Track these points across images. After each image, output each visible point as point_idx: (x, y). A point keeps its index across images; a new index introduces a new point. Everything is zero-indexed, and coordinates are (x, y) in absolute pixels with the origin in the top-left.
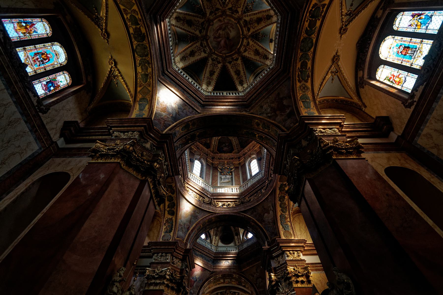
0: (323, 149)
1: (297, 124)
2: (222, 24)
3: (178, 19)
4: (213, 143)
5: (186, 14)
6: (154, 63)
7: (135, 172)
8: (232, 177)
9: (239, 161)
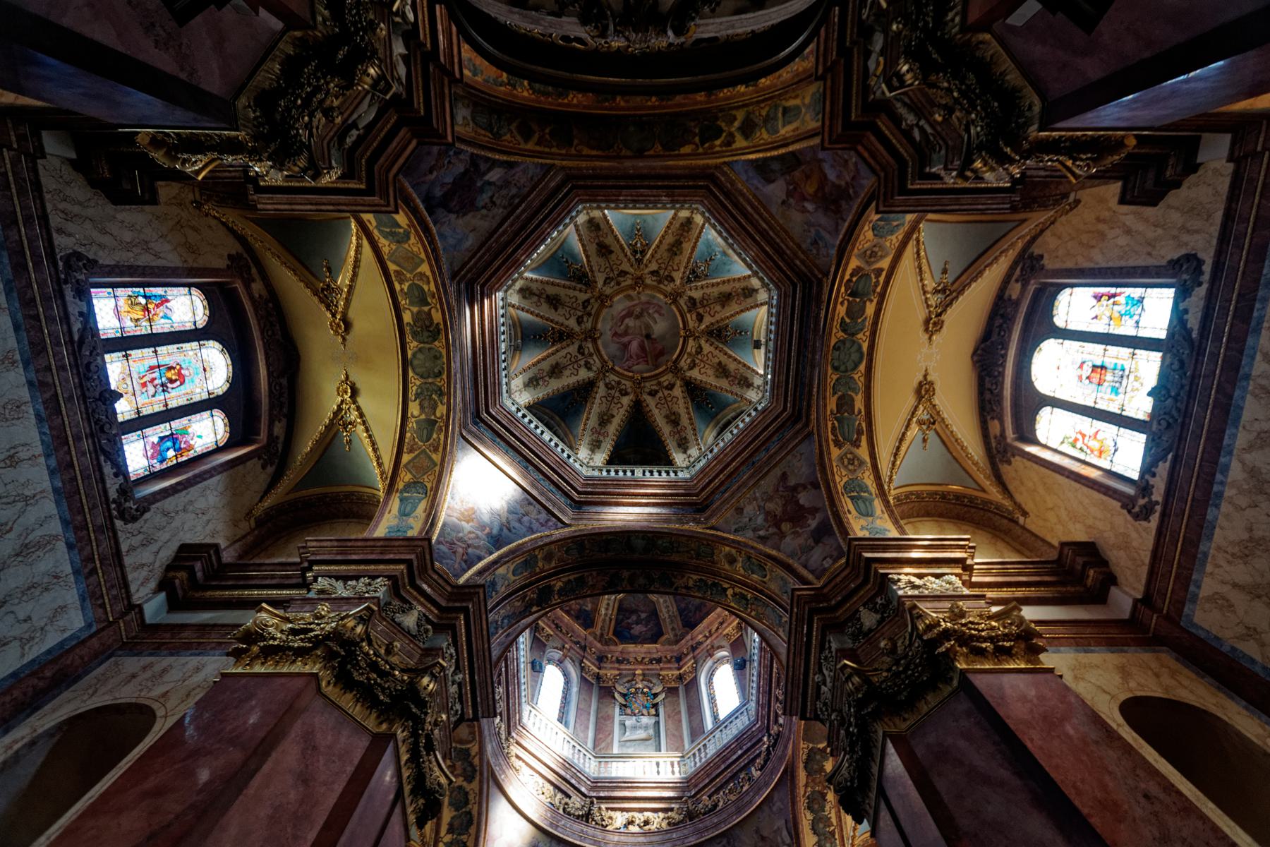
0: (925, 638)
1: (843, 560)
3: (525, 292)
4: (603, 611)
5: (547, 283)
6: (455, 392)
7: (358, 708)
8: (657, 723)
9: (679, 669)
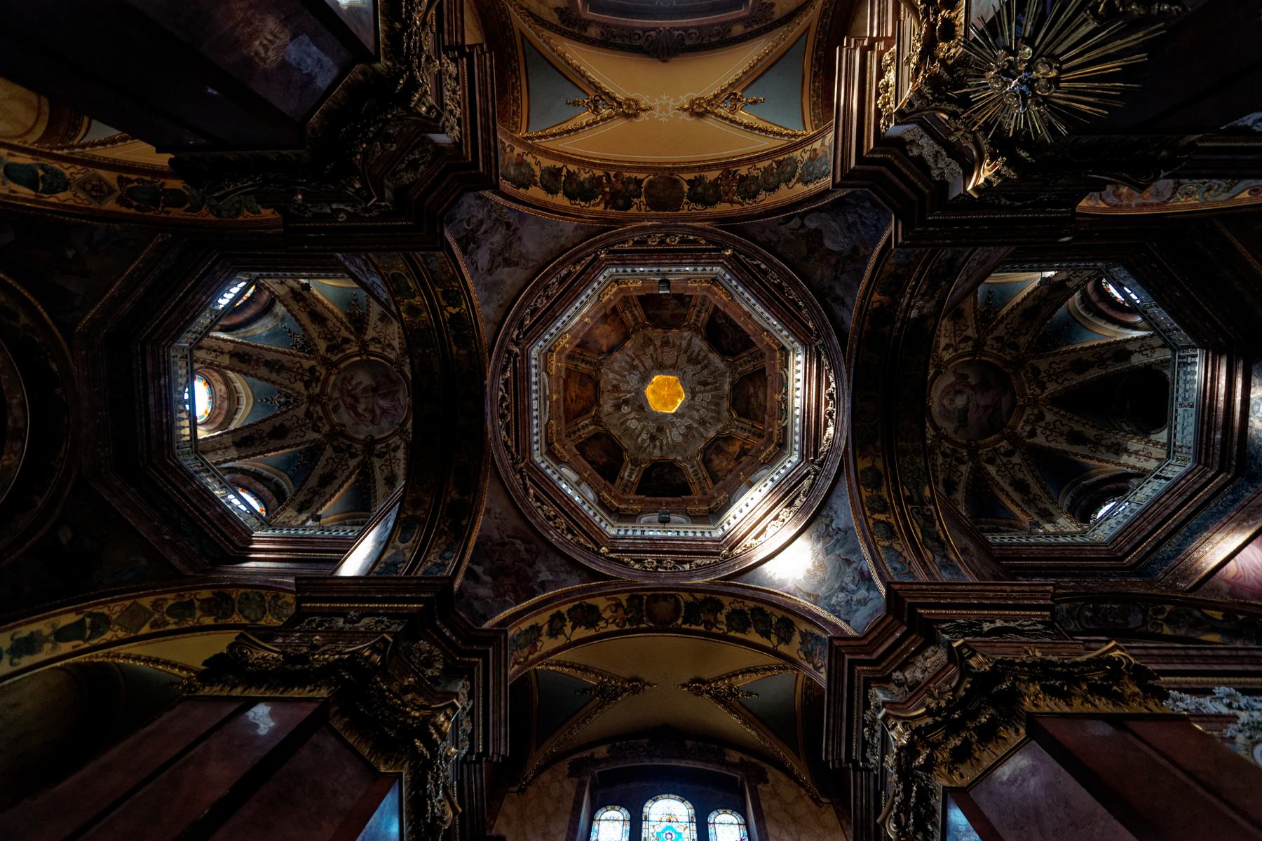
2: (344, 402)
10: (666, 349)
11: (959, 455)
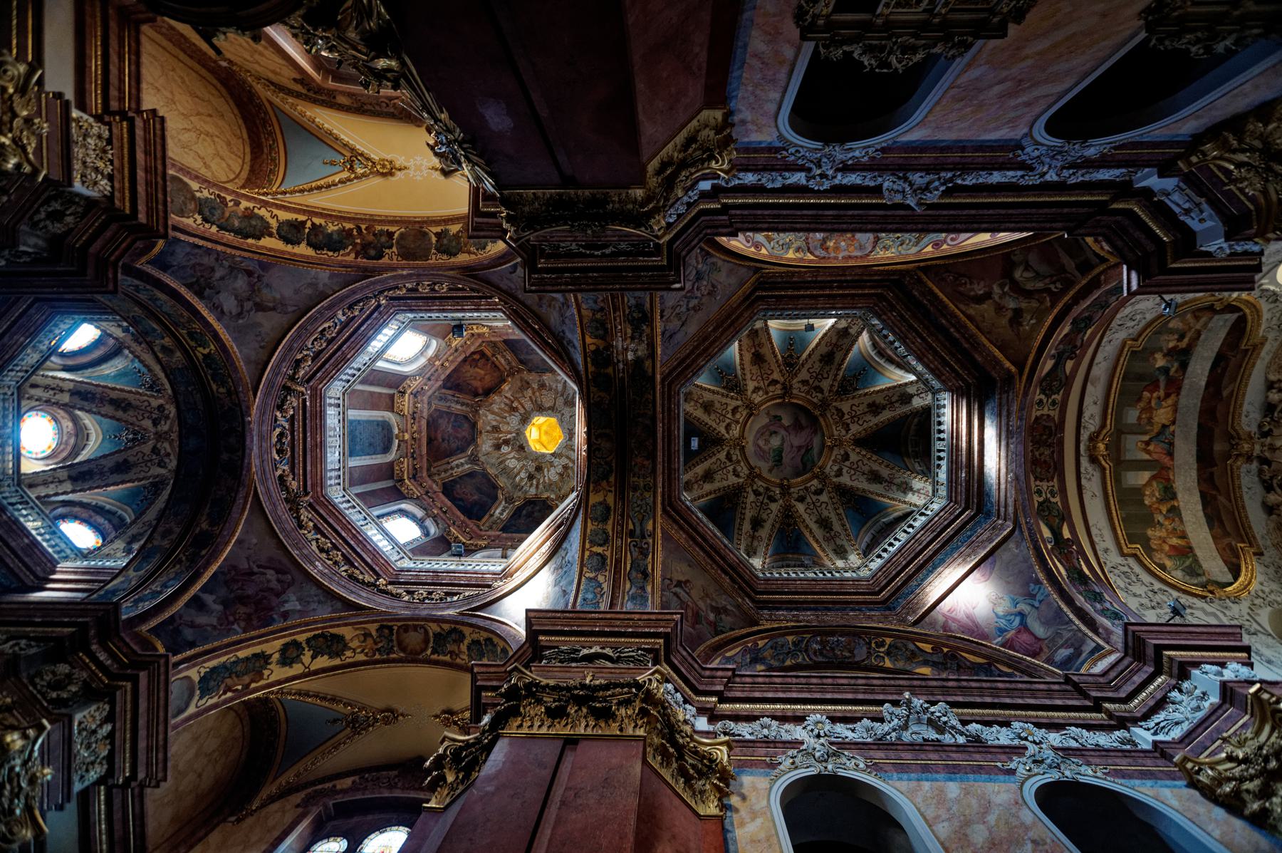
10: (544, 392)
11: (772, 493)
